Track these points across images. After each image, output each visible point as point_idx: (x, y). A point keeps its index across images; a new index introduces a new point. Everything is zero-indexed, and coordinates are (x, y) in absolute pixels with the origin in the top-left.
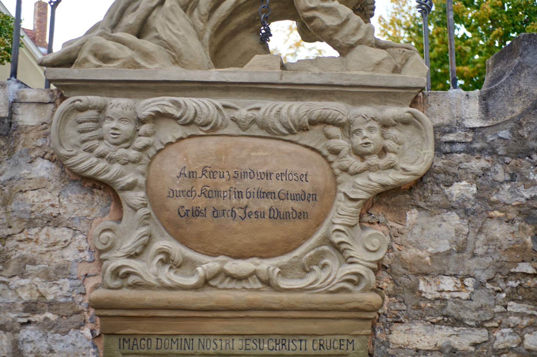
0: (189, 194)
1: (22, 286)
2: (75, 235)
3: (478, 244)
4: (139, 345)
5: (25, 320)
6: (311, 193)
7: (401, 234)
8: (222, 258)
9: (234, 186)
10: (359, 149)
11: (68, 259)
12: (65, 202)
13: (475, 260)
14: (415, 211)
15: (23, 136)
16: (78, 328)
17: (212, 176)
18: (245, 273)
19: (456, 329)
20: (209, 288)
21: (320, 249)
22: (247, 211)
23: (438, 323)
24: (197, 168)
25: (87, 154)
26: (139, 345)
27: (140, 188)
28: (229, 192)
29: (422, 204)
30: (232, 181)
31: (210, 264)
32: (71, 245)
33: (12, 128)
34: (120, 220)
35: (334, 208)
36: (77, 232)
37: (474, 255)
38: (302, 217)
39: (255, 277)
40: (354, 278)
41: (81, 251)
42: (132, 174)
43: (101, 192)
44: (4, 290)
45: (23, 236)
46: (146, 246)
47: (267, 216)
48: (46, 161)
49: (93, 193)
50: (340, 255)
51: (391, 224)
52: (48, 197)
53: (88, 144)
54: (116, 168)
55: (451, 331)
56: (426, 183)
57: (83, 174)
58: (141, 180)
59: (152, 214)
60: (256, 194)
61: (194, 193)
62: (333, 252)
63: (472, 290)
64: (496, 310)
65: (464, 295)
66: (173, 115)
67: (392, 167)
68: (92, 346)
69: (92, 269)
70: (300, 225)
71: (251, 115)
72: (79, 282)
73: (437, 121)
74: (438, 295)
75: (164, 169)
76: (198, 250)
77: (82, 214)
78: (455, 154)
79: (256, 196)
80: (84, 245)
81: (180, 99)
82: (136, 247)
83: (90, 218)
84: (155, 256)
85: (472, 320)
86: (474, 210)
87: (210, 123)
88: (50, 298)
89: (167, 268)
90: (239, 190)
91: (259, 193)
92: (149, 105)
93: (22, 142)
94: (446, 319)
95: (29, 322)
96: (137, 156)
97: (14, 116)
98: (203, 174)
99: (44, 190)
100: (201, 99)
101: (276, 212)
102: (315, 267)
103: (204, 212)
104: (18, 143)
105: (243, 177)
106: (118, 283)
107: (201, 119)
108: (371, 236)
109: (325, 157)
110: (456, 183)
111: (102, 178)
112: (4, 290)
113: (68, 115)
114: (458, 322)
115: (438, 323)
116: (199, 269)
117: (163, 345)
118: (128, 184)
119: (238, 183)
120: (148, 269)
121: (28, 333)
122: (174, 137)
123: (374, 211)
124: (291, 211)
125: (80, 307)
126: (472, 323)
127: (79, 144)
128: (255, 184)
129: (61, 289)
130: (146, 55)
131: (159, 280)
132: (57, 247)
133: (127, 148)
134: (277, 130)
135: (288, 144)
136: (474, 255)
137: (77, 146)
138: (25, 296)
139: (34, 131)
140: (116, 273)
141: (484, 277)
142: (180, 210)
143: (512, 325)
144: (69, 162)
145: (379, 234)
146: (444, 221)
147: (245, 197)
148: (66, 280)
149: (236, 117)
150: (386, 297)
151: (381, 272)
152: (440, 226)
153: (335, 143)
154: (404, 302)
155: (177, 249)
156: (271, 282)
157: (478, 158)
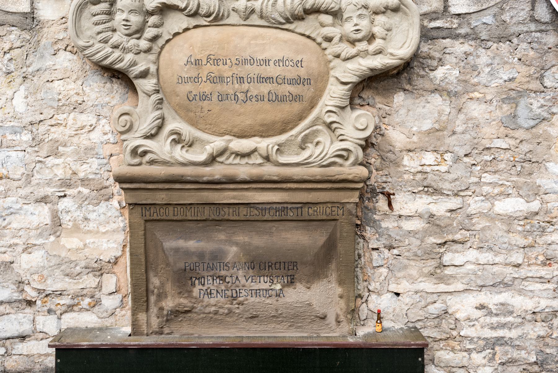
0: (196, 80)
1: (57, 165)
4: (158, 213)
5: (62, 194)
6: (306, 78)
7: (389, 115)
8: (227, 137)
9: (236, 73)
10: (350, 36)
11: (94, 141)
12: (87, 90)
14: (402, 93)
15: (45, 30)
16: (107, 200)
17: (215, 64)
18: (247, 150)
19: (434, 197)
20: (217, 164)
21: (315, 128)
24: (203, 56)
25: (102, 45)
26: (158, 213)
27: (152, 75)
28: (231, 78)
29: (408, 87)
30: (234, 67)
31: (217, 143)
32: (96, 129)
33: (35, 22)
35: (327, 91)
36: (101, 117)
37: (454, 133)
38: (297, 100)
39: (256, 153)
40: (344, 153)
41: (105, 134)
42: (144, 63)
44: (41, 168)
45: (53, 122)
46: (160, 128)
47: (266, 100)
48: (68, 53)
53: (103, 35)
54: (129, 57)
55: (430, 199)
56: (413, 68)
57: (100, 64)
59: (164, 99)
60: (256, 79)
61: (200, 79)
63: (451, 163)
64: (471, 181)
65: (443, 168)
66: (178, 6)
67: (379, 52)
68: (119, 215)
69: (115, 149)
70: (297, 107)
71: (250, 5)
72: (105, 161)
73: (425, 9)
74: (420, 168)
75: (172, 57)
76: (206, 131)
77: (104, 101)
78: (441, 40)
80: (107, 128)
83: (111, 105)
84: (168, 137)
85: (449, 190)
86: (456, 92)
87: (213, 13)
88: (81, 175)
89: (180, 146)
90: (241, 76)
91: (259, 79)
93: (45, 36)
94: (426, 189)
96: (148, 46)
97: (36, 11)
98: (207, 62)
99: (68, 80)
101: (274, 96)
103: (210, 96)
104: (42, 37)
105: (244, 63)
106: (137, 160)
108: (359, 116)
109: (319, 44)
110: (440, 67)
111: (117, 66)
112: (41, 168)
113: (82, 8)
114: (437, 191)
117: (179, 213)
118: (141, 72)
119: (239, 69)
120: (161, 147)
122: (180, 27)
124: (288, 94)
127: (94, 35)
129: (90, 167)
132: (83, 130)
133: (138, 38)
135: (285, 32)
136: (454, 133)
138: (60, 173)
139: (55, 25)
140: (134, 152)
143: (484, 194)
144: (86, 52)
146: (429, 103)
147: (246, 82)
148: (94, 159)
149: (236, 7)
150: (374, 171)
151: (370, 149)
153: (328, 31)
154: (390, 174)
156: (271, 158)
157: (462, 43)
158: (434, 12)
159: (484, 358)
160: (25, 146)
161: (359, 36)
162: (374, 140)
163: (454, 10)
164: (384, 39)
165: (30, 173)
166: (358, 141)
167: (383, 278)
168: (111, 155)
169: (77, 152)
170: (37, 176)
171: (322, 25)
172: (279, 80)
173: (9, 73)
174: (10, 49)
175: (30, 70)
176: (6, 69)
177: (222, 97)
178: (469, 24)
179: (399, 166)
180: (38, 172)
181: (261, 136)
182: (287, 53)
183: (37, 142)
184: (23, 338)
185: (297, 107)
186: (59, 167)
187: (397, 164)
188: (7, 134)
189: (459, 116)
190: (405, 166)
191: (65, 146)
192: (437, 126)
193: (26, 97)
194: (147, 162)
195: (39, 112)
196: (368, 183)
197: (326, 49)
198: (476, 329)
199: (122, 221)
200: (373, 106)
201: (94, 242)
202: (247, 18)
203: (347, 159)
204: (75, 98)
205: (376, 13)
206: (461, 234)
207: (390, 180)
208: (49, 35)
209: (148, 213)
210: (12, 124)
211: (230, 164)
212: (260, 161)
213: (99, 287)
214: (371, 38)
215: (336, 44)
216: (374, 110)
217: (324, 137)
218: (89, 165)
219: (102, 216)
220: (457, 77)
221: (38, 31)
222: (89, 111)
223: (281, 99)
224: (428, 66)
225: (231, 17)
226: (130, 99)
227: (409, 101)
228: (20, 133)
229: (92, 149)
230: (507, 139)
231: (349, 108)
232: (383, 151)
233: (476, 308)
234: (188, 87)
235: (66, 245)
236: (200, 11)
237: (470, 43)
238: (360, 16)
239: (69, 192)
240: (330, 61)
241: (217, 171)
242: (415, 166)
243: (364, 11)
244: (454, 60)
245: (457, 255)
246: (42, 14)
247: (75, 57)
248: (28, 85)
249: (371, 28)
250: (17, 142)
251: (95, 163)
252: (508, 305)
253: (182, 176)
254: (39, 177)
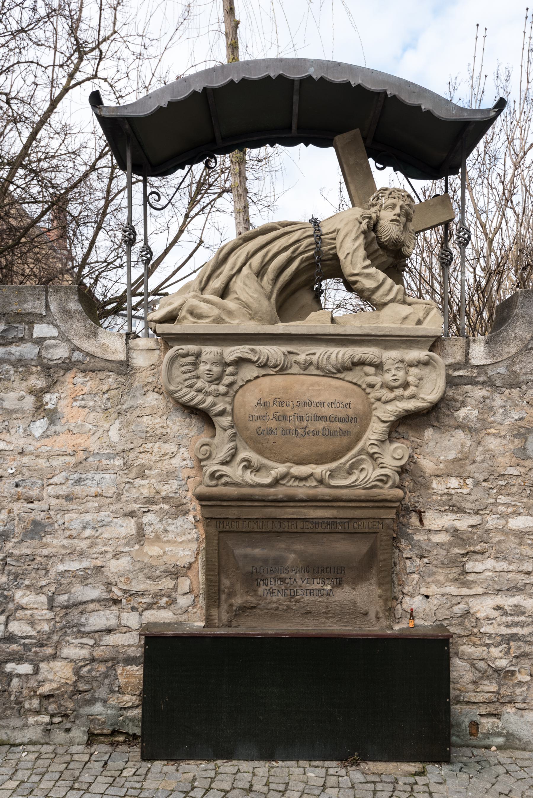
0: (265, 418)
2: (179, 448)
3: (477, 454)
5: (146, 510)
8: (288, 464)
12: (170, 423)
14: (431, 429)
15: (137, 375)
16: (184, 515)
18: (305, 475)
19: (458, 515)
21: (360, 457)
22: (307, 430)
25: (188, 389)
27: (228, 413)
29: (436, 424)
30: (296, 408)
31: (280, 469)
34: (214, 436)
35: (370, 428)
37: (474, 462)
39: (312, 477)
40: (384, 478)
41: (184, 460)
45: (142, 450)
46: (233, 456)
47: (320, 434)
49: (191, 418)
50: (374, 462)
51: (413, 439)
54: (210, 400)
55: (454, 516)
58: (229, 408)
62: (368, 460)
64: (488, 502)
65: (465, 491)
67: (412, 397)
69: (193, 472)
70: (345, 440)
72: (184, 482)
73: (450, 361)
74: (446, 491)
75: (245, 400)
80: (186, 455)
81: (257, 348)
82: (227, 457)
84: (240, 463)
85: (470, 509)
88: (163, 494)
92: (232, 352)
94: (451, 508)
97: (130, 360)
100: (272, 347)
102: (355, 471)
107: (272, 363)
108: (396, 448)
109: (364, 390)
114: (460, 510)
116: (272, 472)
118: (220, 411)
120: (235, 472)
123: (400, 430)
125: (185, 501)
126: (470, 511)
127: (182, 381)
128: (312, 411)
130: (230, 313)
131: (243, 480)
133: (217, 384)
135: (337, 380)
136: (474, 462)
137: (181, 383)
138: (145, 492)
140: (212, 476)
143: (500, 513)
144: (176, 395)
145: (402, 447)
148: (174, 481)
150: (408, 492)
153: (371, 379)
155: (256, 458)
157: (480, 389)
158: (458, 364)
160: (117, 469)
161: (397, 384)
162: (408, 467)
163: (473, 362)
164: (417, 386)
165: (121, 492)
166: (395, 468)
167: (415, 582)
168: (189, 478)
169: (160, 475)
170: (126, 494)
171: (367, 375)
172: (331, 419)
173: (106, 410)
174: (109, 390)
175: (124, 407)
177: (286, 432)
178: (487, 373)
179: (428, 489)
180: (127, 491)
181: (316, 464)
182: (339, 397)
183: (127, 466)
185: (345, 440)
186: (145, 488)
187: (427, 487)
188: (103, 460)
190: (434, 489)
191: (151, 469)
192: (460, 456)
193: (120, 430)
194: (223, 484)
195: (130, 441)
196: (403, 503)
197: (369, 394)
199: (196, 533)
200: (407, 439)
201: (172, 550)
202: (305, 369)
203: (386, 483)
204: (161, 430)
205: (410, 365)
207: (421, 500)
210: (108, 451)
211: (291, 486)
212: (315, 484)
214: (406, 385)
215: (378, 390)
216: (409, 443)
217: (368, 465)
218: (169, 486)
220: (476, 417)
221: (132, 376)
222: (171, 441)
223: (332, 434)
224: (453, 407)
225: (293, 368)
226: (205, 432)
227: (437, 436)
228: (114, 459)
229: (173, 472)
231: (388, 442)
232: (415, 476)
234: (258, 423)
235: (149, 552)
236: (268, 363)
237: (487, 388)
238: (397, 368)
240: (373, 404)
241: (280, 491)
242: (442, 489)
243: (401, 365)
244: (474, 402)
247: (161, 397)
248: (122, 420)
249: (406, 378)
250: (111, 466)
251: (175, 484)
253: (252, 496)
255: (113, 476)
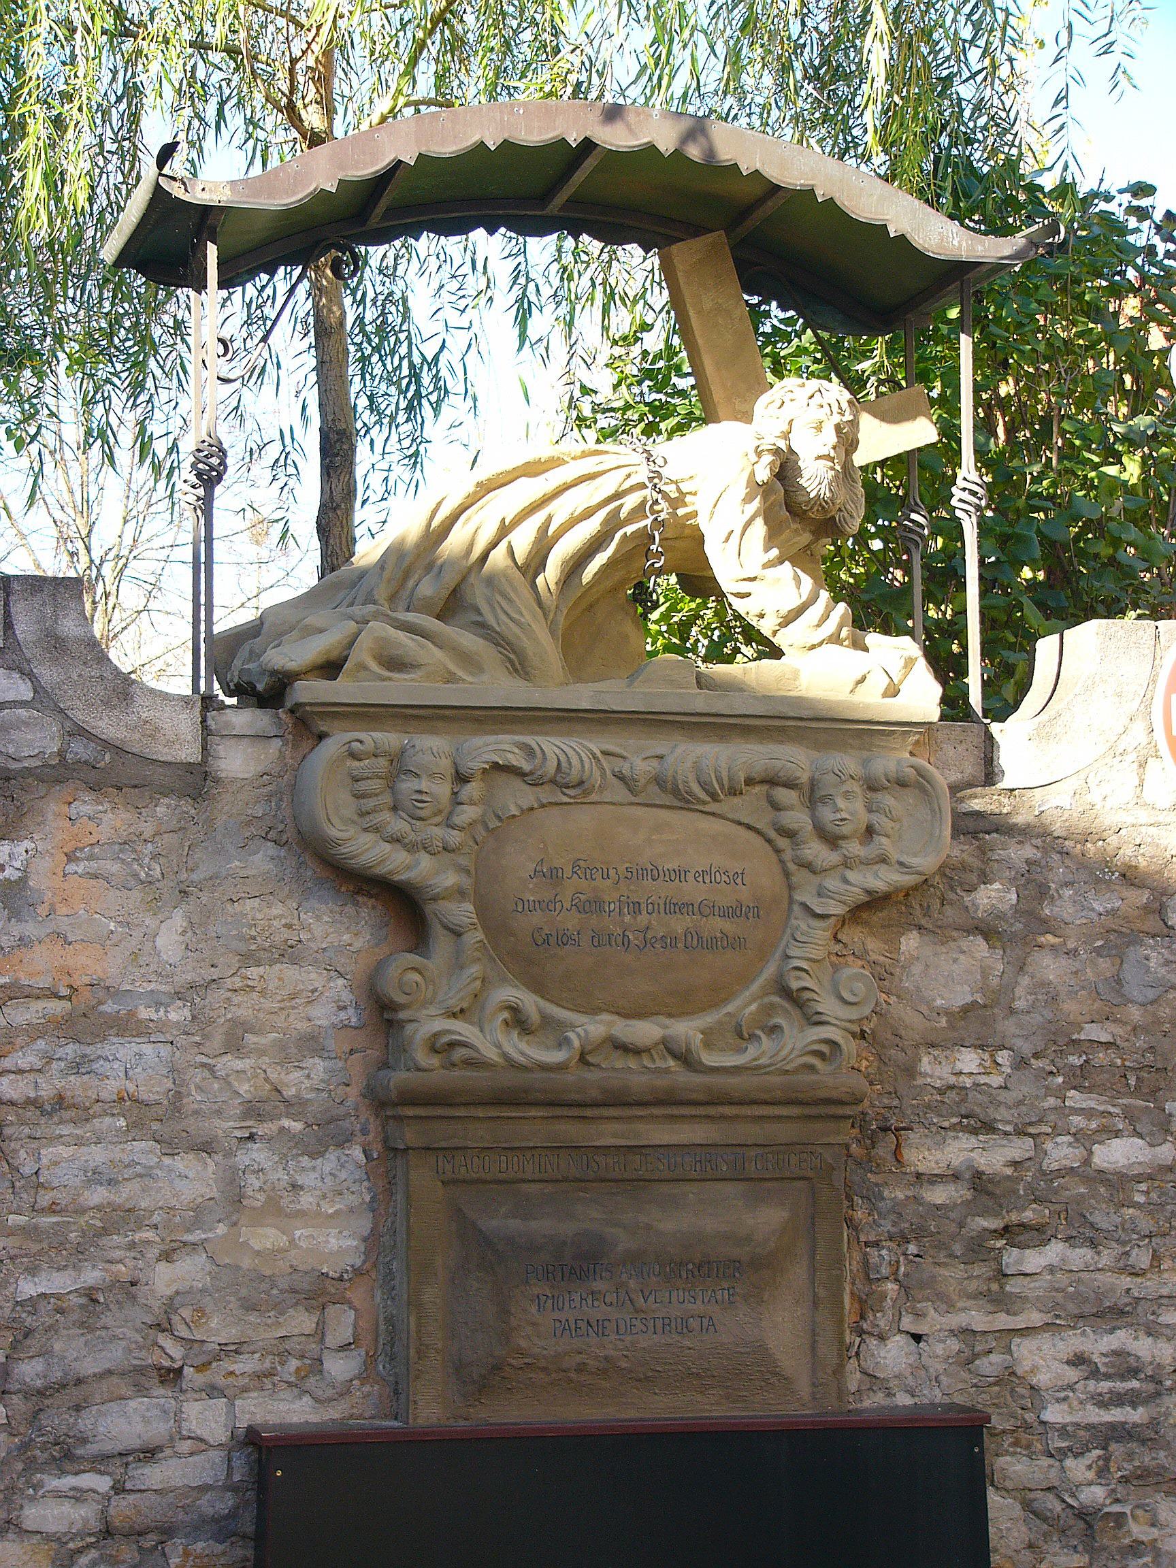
3: (1019, 991)
13: (1012, 1019)
19: (981, 1137)
23: (953, 1127)
31: (595, 1027)
37: (1012, 1011)
40: (825, 1048)
43: (371, 902)
45: (237, 982)
48: (269, 844)
49: (357, 904)
52: (276, 911)
60: (662, 907)
63: (1009, 1071)
65: (996, 1080)
74: (953, 1080)
79: (662, 911)
83: (351, 948)
85: (1008, 1122)
95: (251, 1138)
109: (769, 841)
115: (953, 1127)
121: (257, 1154)
124: (719, 935)
126: (1009, 1128)
129: (308, 1076)
131: (505, 1055)
134: (691, 794)
135: (711, 818)
141: (1026, 1049)
142: (536, 935)
143: (1073, 1130)
152: (955, 961)
155: (530, 1002)
159: (1089, 1467)
166: (848, 1025)
176: (147, 874)
177: (600, 939)
181: (670, 1015)
184: (150, 1453)
188: (142, 1008)
189: (1019, 979)
190: (925, 1075)
193: (184, 933)
198: (1070, 1407)
206: (1034, 1210)
208: (229, 808)
209: (448, 1167)
210: (152, 986)
213: (320, 1333)
219: (328, 1179)
230: (1108, 1023)
233: (1068, 1363)
239: (262, 1129)
245: (1027, 1251)
246: (223, 766)
252: (1129, 1354)
254: (199, 1098)
255: (165, 1050)
